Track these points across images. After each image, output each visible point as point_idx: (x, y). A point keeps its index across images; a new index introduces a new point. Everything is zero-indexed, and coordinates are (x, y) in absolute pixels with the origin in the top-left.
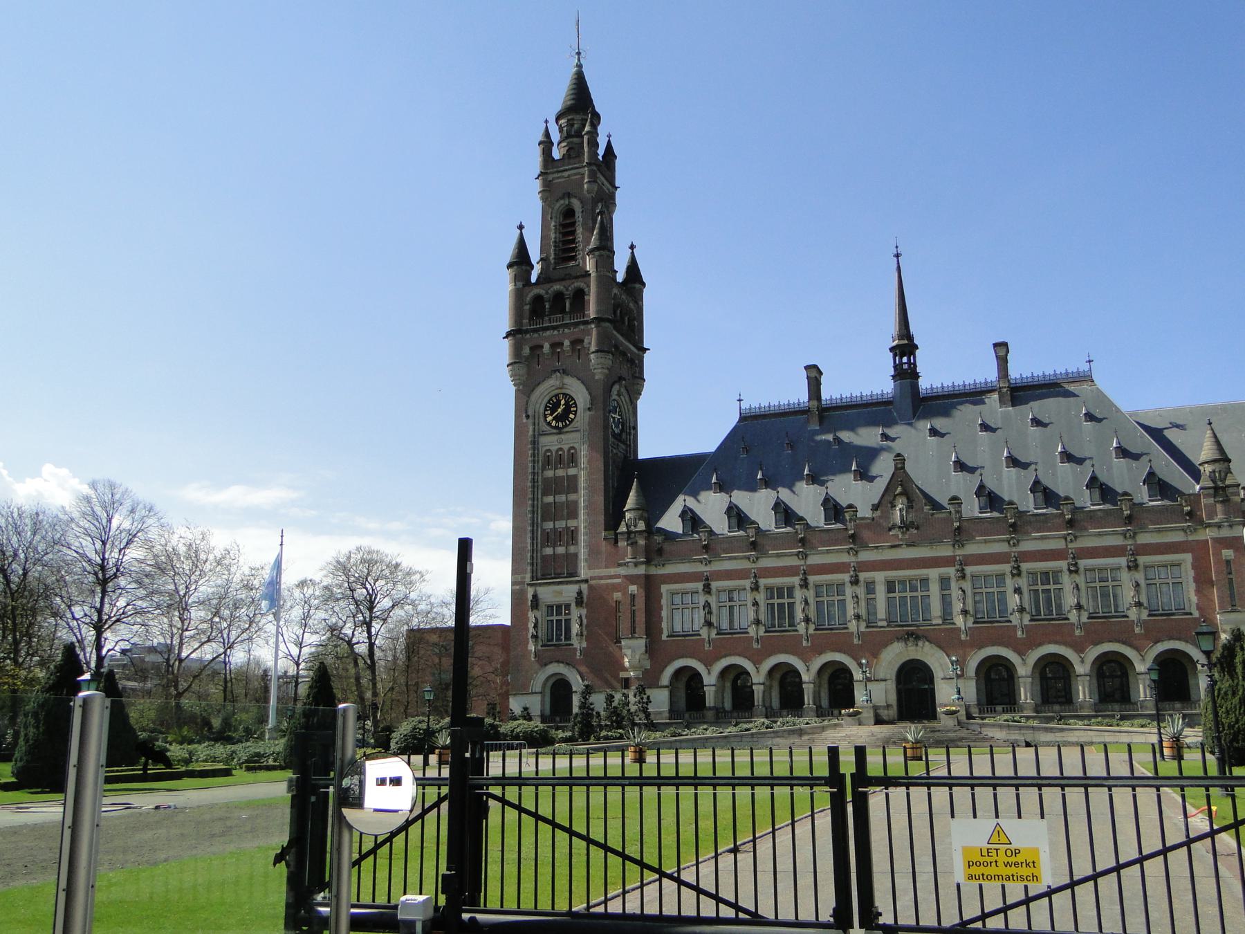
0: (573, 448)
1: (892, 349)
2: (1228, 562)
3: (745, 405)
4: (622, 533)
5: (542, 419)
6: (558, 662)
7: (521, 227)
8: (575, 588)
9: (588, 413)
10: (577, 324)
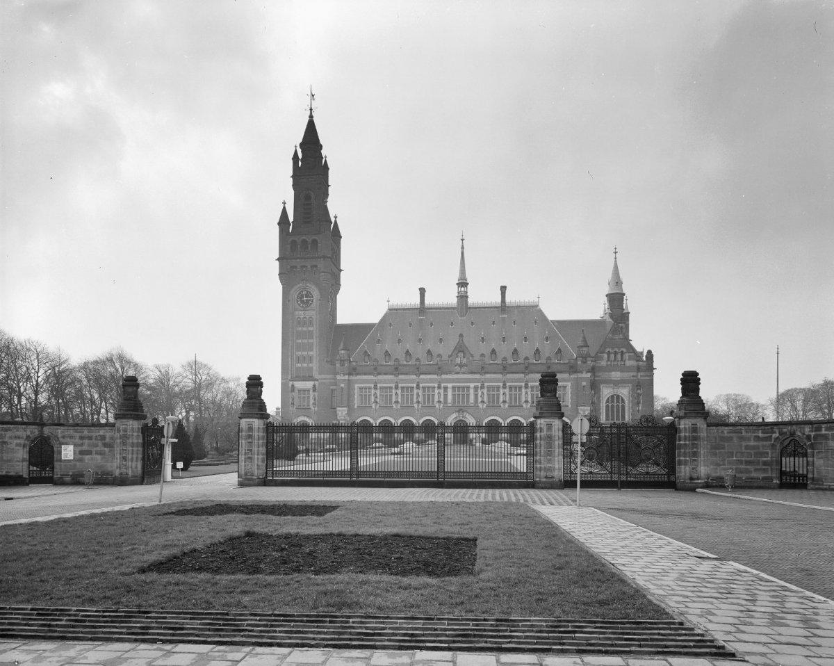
1: (457, 284)
2: (584, 387)
6: (304, 416)
7: (284, 203)
8: (312, 383)
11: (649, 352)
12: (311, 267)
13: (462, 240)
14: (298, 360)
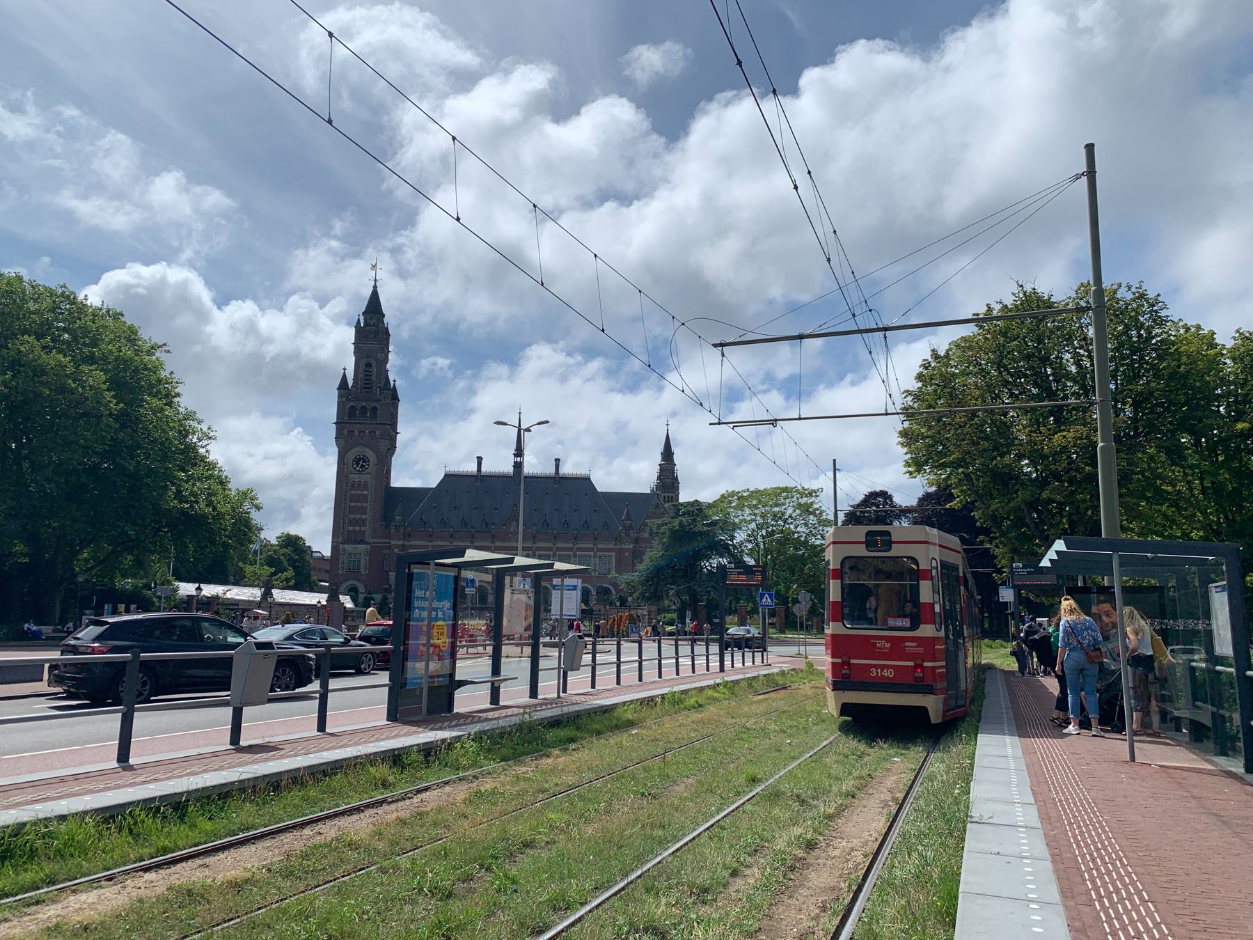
8: (364, 546)
14: (351, 523)
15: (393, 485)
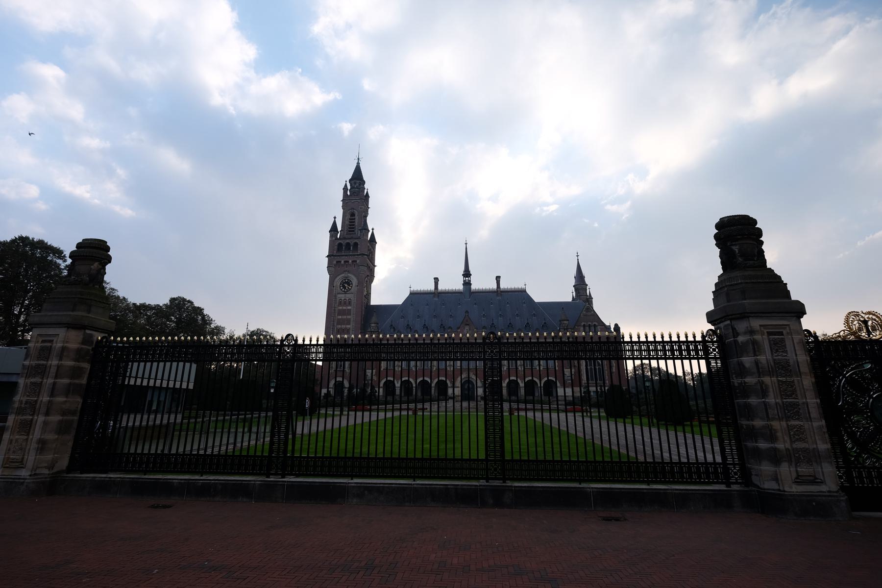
0: (349, 299)
3: (412, 289)
4: (369, 331)
5: (339, 289)
7: (335, 218)
9: (357, 287)
10: (354, 255)
11: (616, 325)
12: (352, 261)
13: (466, 244)
15: (372, 303)
